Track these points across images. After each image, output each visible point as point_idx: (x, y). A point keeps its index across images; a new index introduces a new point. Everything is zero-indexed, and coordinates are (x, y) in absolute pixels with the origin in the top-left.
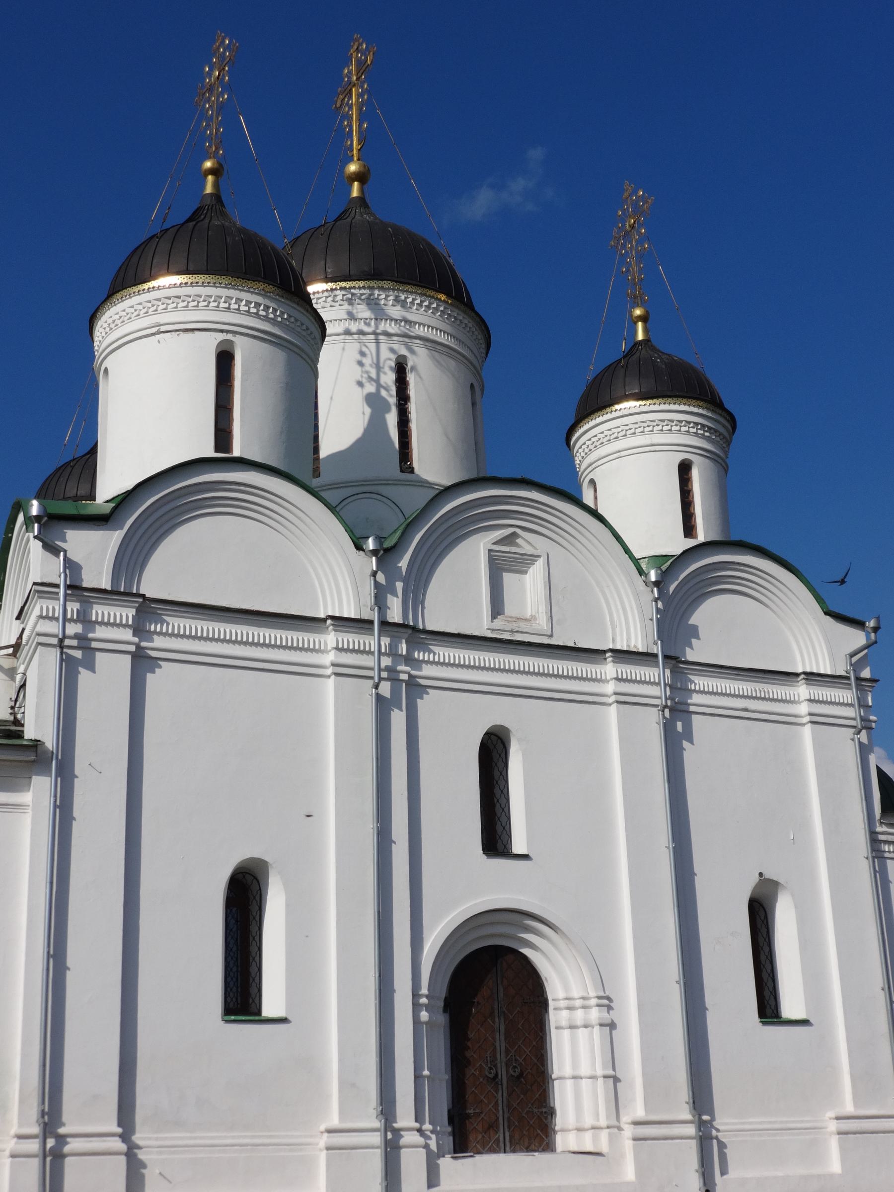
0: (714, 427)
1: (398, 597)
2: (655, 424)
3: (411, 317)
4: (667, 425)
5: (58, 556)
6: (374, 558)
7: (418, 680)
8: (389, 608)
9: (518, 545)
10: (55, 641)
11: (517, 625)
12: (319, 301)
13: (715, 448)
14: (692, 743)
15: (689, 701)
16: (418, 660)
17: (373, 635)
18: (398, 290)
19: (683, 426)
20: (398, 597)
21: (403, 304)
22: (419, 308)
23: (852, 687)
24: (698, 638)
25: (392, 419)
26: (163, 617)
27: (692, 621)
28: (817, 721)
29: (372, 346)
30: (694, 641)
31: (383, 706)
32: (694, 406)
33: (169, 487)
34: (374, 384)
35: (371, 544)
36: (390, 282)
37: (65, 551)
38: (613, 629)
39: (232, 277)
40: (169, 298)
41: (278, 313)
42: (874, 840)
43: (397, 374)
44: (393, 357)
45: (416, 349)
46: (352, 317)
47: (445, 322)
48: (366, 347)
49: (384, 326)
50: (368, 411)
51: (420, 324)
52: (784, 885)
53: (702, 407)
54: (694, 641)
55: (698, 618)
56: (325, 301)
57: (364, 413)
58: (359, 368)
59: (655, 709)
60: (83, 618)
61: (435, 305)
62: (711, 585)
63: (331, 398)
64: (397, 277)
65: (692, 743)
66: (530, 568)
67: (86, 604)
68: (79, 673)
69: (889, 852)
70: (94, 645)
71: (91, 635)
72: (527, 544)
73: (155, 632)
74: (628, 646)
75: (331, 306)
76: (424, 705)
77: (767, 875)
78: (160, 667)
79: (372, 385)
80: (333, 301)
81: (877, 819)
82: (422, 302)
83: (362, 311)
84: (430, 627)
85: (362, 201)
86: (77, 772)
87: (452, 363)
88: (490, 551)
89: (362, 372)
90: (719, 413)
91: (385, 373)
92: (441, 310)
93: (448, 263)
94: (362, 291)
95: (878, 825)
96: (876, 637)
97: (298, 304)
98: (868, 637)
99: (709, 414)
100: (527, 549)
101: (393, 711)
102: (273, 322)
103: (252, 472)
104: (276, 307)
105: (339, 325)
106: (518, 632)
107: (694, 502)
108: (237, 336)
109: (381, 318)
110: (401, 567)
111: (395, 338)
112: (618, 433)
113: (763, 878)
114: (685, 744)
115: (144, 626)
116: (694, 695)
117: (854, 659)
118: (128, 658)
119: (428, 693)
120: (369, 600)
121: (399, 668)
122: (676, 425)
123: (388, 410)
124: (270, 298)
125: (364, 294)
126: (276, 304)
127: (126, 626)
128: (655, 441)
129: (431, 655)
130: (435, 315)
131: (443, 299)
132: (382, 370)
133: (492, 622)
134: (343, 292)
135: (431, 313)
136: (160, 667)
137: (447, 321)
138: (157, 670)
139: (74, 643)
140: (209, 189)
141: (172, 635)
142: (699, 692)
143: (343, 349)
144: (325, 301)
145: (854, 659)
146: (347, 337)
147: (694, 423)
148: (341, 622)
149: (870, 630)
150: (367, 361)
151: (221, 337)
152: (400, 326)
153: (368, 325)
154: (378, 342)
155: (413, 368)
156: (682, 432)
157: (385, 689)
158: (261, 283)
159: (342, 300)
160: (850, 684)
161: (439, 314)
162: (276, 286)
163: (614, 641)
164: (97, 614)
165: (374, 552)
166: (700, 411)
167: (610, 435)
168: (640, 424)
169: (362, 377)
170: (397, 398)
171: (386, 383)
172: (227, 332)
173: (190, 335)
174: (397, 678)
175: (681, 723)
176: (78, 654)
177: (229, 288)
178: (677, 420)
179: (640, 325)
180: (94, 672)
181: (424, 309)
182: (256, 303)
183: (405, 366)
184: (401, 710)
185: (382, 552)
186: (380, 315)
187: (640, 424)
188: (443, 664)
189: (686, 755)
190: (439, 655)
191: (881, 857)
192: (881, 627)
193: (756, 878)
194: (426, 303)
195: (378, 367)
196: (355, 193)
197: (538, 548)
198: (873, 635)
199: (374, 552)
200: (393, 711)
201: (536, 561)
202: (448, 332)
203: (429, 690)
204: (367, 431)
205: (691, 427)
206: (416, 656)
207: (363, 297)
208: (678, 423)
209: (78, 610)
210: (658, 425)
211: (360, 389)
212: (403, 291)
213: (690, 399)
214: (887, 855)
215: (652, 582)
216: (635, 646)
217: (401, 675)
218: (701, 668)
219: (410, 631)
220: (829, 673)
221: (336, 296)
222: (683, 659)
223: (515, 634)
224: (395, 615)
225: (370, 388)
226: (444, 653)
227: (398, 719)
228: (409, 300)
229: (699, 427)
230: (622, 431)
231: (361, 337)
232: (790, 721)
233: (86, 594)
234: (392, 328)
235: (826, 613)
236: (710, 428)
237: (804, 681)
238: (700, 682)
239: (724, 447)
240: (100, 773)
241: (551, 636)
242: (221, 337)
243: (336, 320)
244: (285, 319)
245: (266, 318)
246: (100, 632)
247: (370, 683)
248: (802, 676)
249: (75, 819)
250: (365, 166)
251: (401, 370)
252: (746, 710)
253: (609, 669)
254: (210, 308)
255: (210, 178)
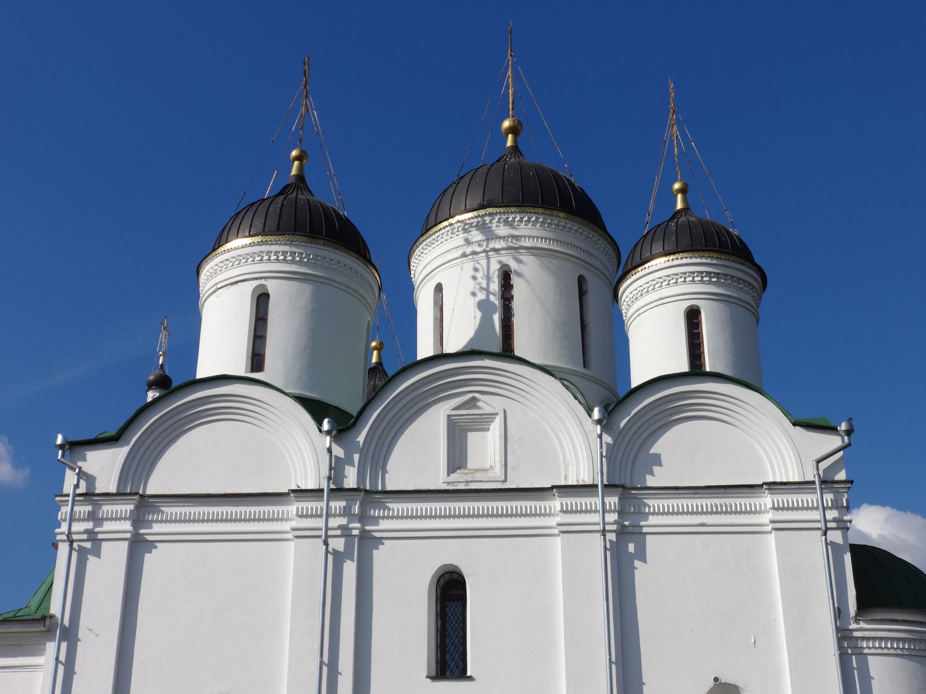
0: (721, 272)
1: (355, 467)
2: (662, 280)
3: (516, 233)
4: (673, 279)
5: (75, 470)
6: (328, 438)
7: (372, 533)
8: (346, 477)
9: (479, 408)
10: (64, 537)
11: (472, 476)
12: (444, 236)
13: (727, 290)
14: (645, 562)
15: (642, 523)
16: (374, 517)
17: (323, 501)
18: (500, 213)
19: (696, 276)
20: (355, 467)
21: (506, 222)
22: (519, 223)
23: (817, 490)
24: (661, 465)
25: (497, 318)
26: (161, 508)
27: (652, 451)
28: (780, 527)
29: (484, 262)
30: (655, 469)
31: (339, 558)
32: (696, 258)
33: (171, 406)
34: (485, 292)
35: (326, 425)
36: (491, 208)
37: (80, 468)
38: (566, 468)
39: (262, 236)
40: (222, 262)
41: (304, 256)
42: (844, 636)
43: (503, 281)
44: (498, 266)
45: (521, 257)
46: (468, 242)
47: (545, 230)
48: (479, 263)
49: (493, 244)
50: (479, 314)
51: (522, 236)
52: (743, 688)
53: (705, 257)
54: (655, 469)
55: (660, 447)
56: (447, 235)
57: (475, 317)
58: (472, 282)
59: (599, 535)
60: (92, 516)
61: (534, 219)
62: (671, 415)
63: (453, 309)
64: (502, 203)
65: (645, 562)
66: (490, 425)
67: (97, 506)
68: (88, 559)
69: (869, 648)
70: (100, 536)
71: (97, 530)
72: (487, 404)
73: (153, 521)
74: (578, 481)
75: (451, 238)
76: (379, 556)
77: (724, 679)
78: (156, 547)
79: (483, 293)
80: (452, 233)
81: (851, 616)
82: (522, 218)
83: (476, 236)
84: (389, 487)
85: (515, 148)
86: (80, 636)
87: (555, 262)
88: (449, 416)
89: (475, 284)
90: (725, 259)
91: (493, 282)
92: (541, 222)
93: (569, 181)
94: (472, 221)
95: (852, 622)
96: (849, 439)
97: (324, 245)
98: (843, 440)
99: (714, 262)
100: (487, 409)
101: (345, 562)
102: (300, 263)
103: (236, 385)
104: (302, 251)
105: (457, 251)
106: (472, 481)
107: (703, 342)
108: (268, 280)
109: (488, 238)
110: (359, 441)
111: (503, 252)
112: (637, 294)
113: (719, 682)
114: (637, 563)
115: (144, 517)
116: (650, 517)
117: (824, 465)
118: (125, 544)
119: (383, 544)
120: (325, 472)
121: (351, 526)
122: (681, 277)
123: (495, 313)
124: (295, 245)
125: (473, 223)
126: (303, 250)
127: (125, 519)
128: (663, 295)
129: (386, 512)
130: (535, 227)
131: (540, 212)
132: (491, 280)
133: (448, 475)
134: (459, 224)
135: (532, 225)
136: (156, 547)
137: (548, 229)
138: (153, 550)
139: (85, 537)
140: (294, 172)
141: (166, 521)
142: (654, 514)
143: (462, 269)
144: (447, 235)
145: (824, 465)
146: (464, 259)
147: (698, 272)
148: (301, 493)
149: (843, 434)
150: (479, 275)
151: (256, 283)
152: (504, 241)
153: (480, 245)
154: (488, 258)
155: (519, 274)
156: (687, 283)
157: (338, 544)
158: (287, 236)
159: (458, 231)
160: (815, 488)
161: (539, 224)
162: (303, 236)
163: (566, 477)
164: (103, 512)
165: (328, 433)
166: (704, 260)
167: (633, 297)
168: (651, 283)
169: (475, 288)
170: (503, 300)
171: (494, 290)
172: (261, 278)
173: (235, 286)
174: (350, 534)
175: (633, 544)
176: (88, 545)
177: (261, 245)
178: (681, 273)
179: (679, 196)
180: (99, 556)
181: (524, 224)
182: (282, 251)
183: (510, 273)
184: (354, 561)
185: (334, 432)
186: (490, 236)
187: (651, 283)
188: (397, 517)
189: (637, 573)
190: (393, 510)
191: (860, 654)
192: (855, 430)
193: (711, 683)
194: (526, 219)
195: (488, 278)
196: (510, 142)
197: (495, 407)
198: (846, 437)
199: (328, 433)
200: (345, 562)
201: (495, 418)
202: (550, 237)
203: (384, 541)
204: (477, 333)
205: (696, 276)
206: (372, 514)
207: (474, 224)
208: (682, 275)
209: (89, 511)
210: (665, 281)
211: (473, 298)
212: (504, 213)
213: (713, 252)
214: (866, 651)
215: (595, 420)
216: (583, 481)
217: (353, 531)
218: (654, 492)
219: (362, 494)
220: (797, 480)
221: (455, 228)
222: (639, 486)
223: (470, 483)
224: (351, 479)
225: (482, 296)
226: (397, 507)
227: (350, 569)
228: (510, 219)
229: (704, 275)
230: (639, 291)
231: (475, 256)
232: (754, 531)
233: (94, 498)
234: (498, 245)
235: (795, 424)
236: (717, 275)
237: (766, 491)
238: (654, 503)
239: (741, 288)
240: (98, 635)
241: (505, 480)
242: (256, 283)
243: (454, 248)
244: (312, 259)
245: (293, 261)
246: (108, 526)
247: (320, 542)
248: (765, 486)
249: (75, 673)
250: (514, 121)
251: (506, 277)
252: (703, 525)
253: (767, 500)
254: (248, 263)
255: (296, 163)
